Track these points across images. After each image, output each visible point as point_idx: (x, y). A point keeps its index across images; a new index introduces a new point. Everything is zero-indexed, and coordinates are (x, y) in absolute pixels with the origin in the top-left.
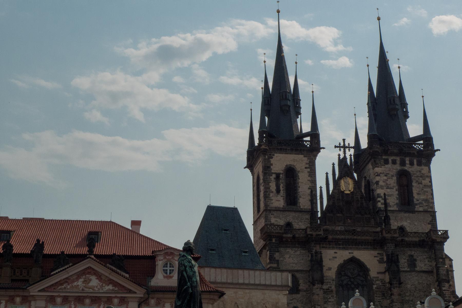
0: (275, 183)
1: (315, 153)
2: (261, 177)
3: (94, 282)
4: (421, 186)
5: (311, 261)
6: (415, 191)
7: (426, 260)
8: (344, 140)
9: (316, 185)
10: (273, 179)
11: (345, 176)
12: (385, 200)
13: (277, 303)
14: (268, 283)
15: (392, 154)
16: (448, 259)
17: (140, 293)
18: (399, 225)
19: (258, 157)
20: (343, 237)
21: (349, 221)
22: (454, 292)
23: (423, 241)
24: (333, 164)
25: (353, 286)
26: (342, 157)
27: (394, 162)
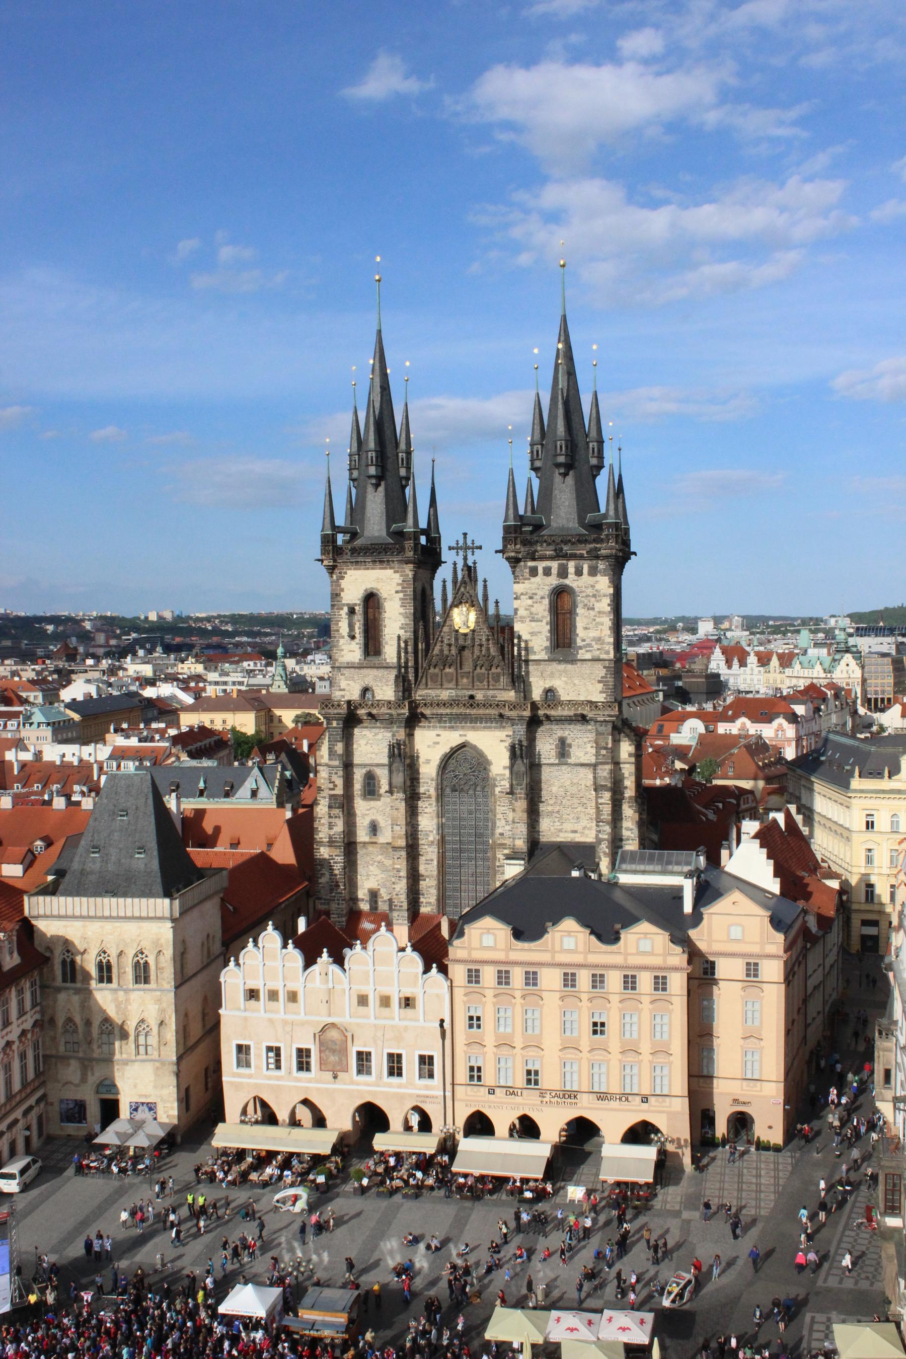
0: (346, 621)
4: (592, 613)
6: (580, 623)
7: (589, 745)
8: (465, 534)
11: (461, 603)
13: (158, 940)
14: (144, 914)
15: (543, 558)
16: (627, 743)
18: (547, 686)
20: (448, 711)
21: (465, 680)
24: (444, 581)
25: (466, 788)
26: (460, 566)
27: (547, 572)
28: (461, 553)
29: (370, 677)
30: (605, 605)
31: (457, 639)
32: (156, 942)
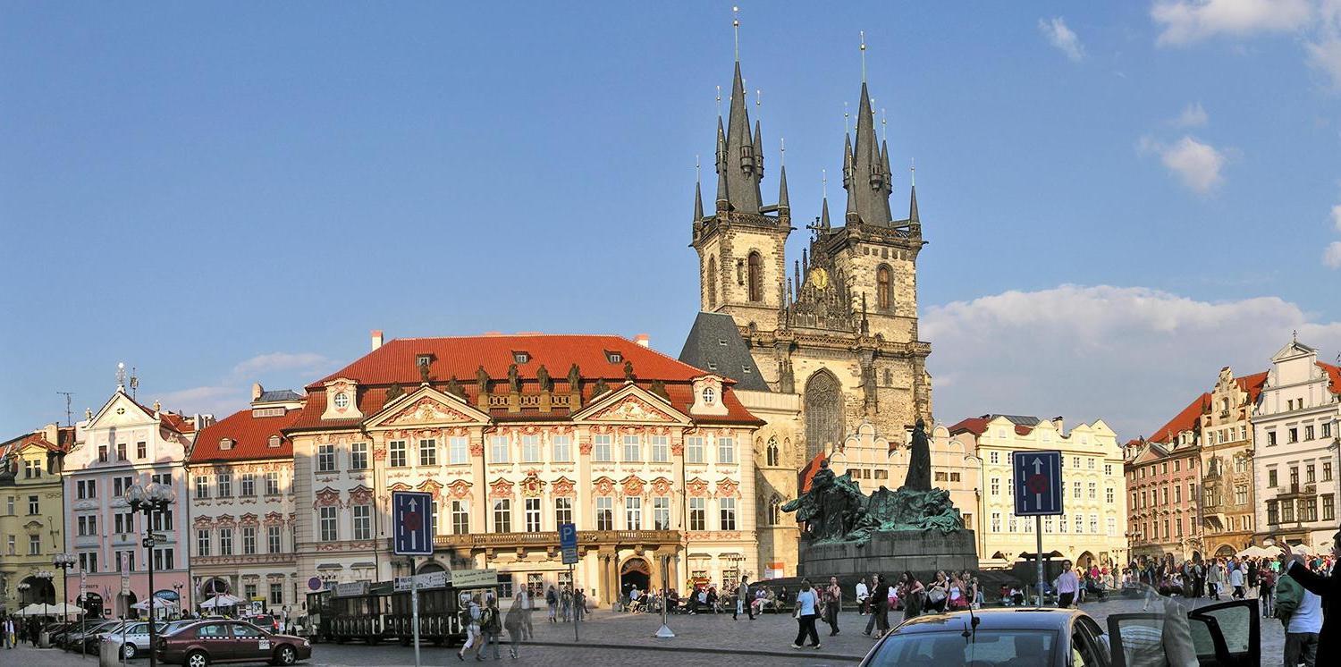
1: (784, 235)
2: (718, 263)
3: (637, 410)
5: (781, 371)
6: (896, 292)
9: (784, 275)
10: (734, 266)
12: (864, 300)
14: (779, 407)
17: (685, 421)
18: (877, 332)
19: (711, 235)
22: (930, 414)
23: (903, 354)
24: (805, 250)
26: (815, 239)
27: (875, 253)
28: (815, 231)
29: (754, 316)
30: (910, 281)
31: (815, 293)
32: (785, 431)
